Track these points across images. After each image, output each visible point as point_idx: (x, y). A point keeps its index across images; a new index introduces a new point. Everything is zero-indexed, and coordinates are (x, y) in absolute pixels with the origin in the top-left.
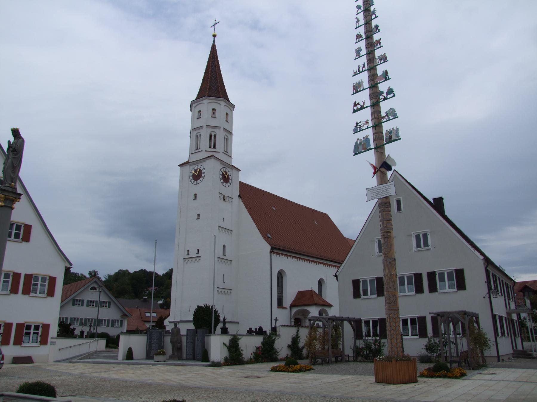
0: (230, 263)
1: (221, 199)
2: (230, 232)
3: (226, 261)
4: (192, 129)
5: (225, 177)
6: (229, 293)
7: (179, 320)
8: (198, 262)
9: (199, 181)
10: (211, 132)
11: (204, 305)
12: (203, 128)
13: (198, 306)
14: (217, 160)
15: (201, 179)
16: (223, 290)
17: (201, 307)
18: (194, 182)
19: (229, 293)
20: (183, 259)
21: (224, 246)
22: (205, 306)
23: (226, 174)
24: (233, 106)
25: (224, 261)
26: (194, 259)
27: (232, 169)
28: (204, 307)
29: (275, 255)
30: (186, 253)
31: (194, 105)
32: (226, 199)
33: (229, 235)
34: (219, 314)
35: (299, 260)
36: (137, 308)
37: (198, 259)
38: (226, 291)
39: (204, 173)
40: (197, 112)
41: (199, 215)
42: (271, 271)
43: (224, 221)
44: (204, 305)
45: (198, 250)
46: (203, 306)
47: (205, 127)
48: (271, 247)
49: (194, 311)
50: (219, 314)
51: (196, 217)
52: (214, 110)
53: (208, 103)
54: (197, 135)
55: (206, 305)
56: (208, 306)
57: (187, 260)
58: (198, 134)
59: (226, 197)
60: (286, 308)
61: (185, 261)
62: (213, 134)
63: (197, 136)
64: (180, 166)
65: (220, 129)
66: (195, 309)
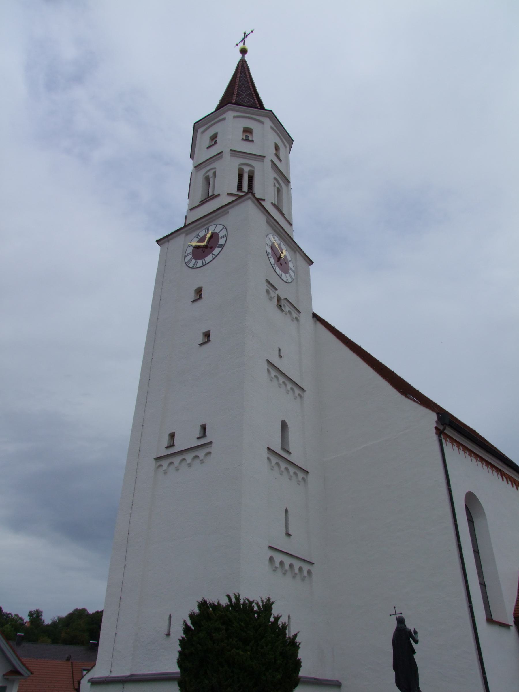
0: (303, 479)
1: (271, 299)
2: (297, 391)
3: (292, 470)
4: (195, 167)
5: (280, 258)
6: (305, 573)
7: (128, 673)
8: (202, 462)
9: (208, 258)
10: (240, 165)
11: (228, 596)
12: (221, 158)
13: (203, 605)
14: (257, 206)
15: (216, 251)
16: (288, 561)
17: (216, 607)
18: (196, 263)
19: (305, 573)
20: (154, 462)
21: (284, 426)
22: (234, 600)
23: (282, 253)
24: (290, 141)
25: (286, 469)
26: (189, 457)
27: (295, 252)
28: (227, 606)
29: (449, 444)
30: (165, 441)
31: (200, 131)
32: (284, 306)
33: (295, 398)
34: (295, 636)
35: (500, 477)
36: (68, 659)
37: (201, 453)
38: (297, 565)
39: (223, 237)
40: (209, 138)
41: (207, 335)
42: (450, 490)
43: (280, 356)
44: (228, 596)
45: (204, 428)
46: (224, 602)
47: (227, 155)
48: (437, 414)
49: (186, 624)
50: (295, 636)
51: (200, 339)
52: (247, 131)
53: (235, 117)
54: (207, 174)
55: (237, 598)
56: (244, 604)
57: (165, 463)
58: (211, 174)
59: (283, 303)
60: (507, 626)
61: (161, 465)
62: (246, 169)
63: (207, 180)
64: (160, 243)
65: (263, 161)
66: (188, 613)
